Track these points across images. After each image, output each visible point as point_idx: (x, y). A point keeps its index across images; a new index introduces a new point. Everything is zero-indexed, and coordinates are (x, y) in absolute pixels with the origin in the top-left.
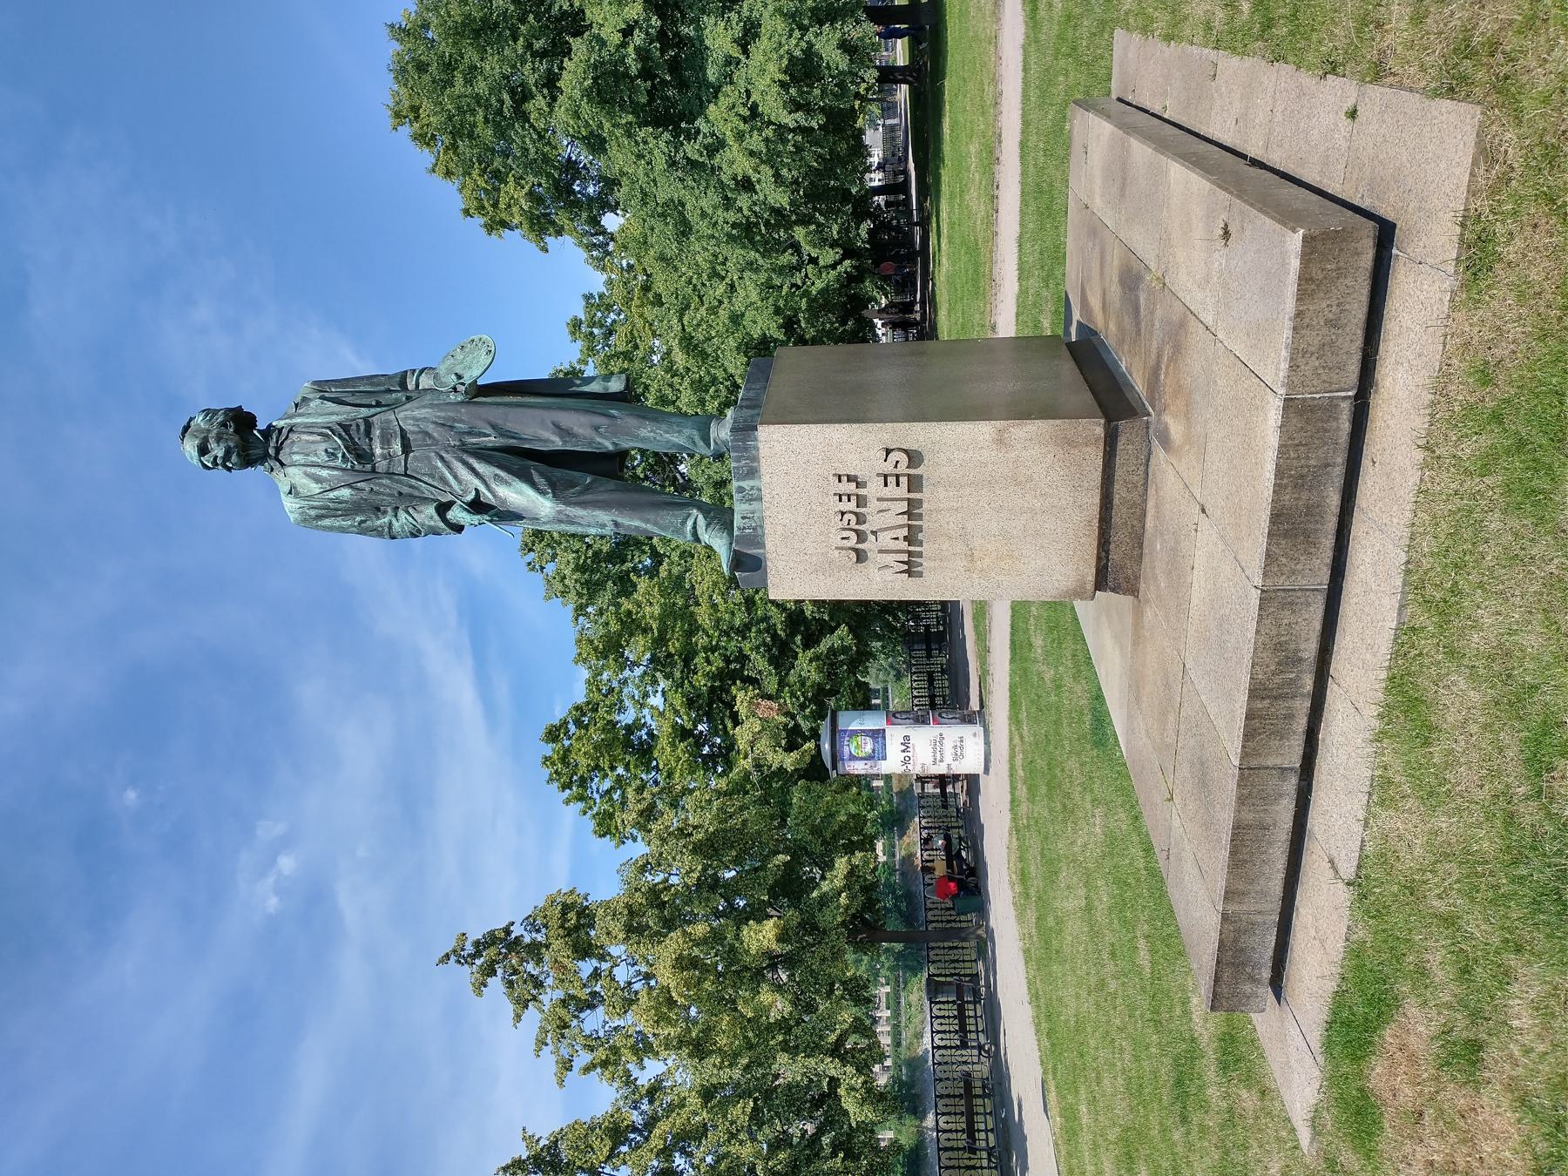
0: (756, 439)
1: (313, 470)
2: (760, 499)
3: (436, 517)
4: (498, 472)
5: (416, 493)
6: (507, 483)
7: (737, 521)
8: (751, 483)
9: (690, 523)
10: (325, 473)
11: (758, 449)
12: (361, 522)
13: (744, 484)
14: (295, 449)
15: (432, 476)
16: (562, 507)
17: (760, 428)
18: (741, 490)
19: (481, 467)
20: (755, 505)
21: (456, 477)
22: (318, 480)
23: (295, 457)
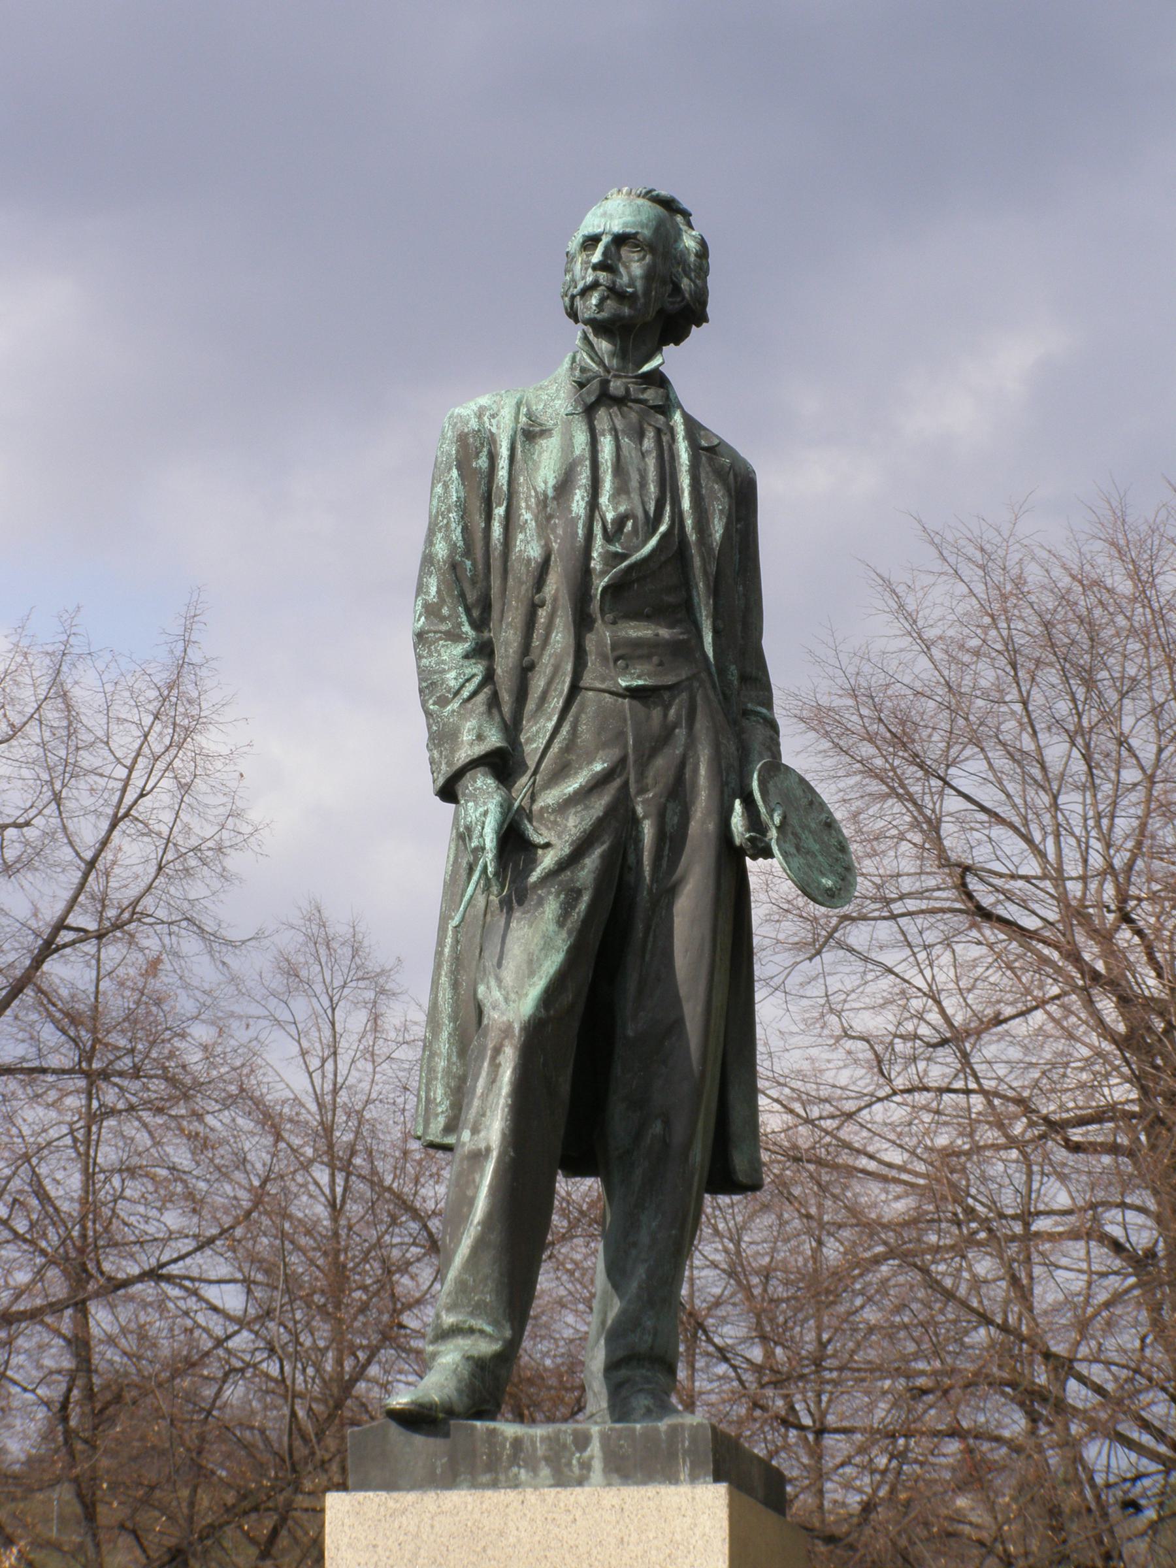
0: (693, 1479)
1: (583, 477)
2: (561, 1480)
3: (479, 750)
4: (586, 898)
5: (531, 705)
6: (561, 921)
8: (597, 1465)
9: (478, 1323)
10: (578, 503)
11: (672, 1479)
13: (595, 1448)
14: (625, 441)
15: (568, 748)
17: (722, 1489)
19: (591, 862)
20: (545, 1472)
22: (564, 487)
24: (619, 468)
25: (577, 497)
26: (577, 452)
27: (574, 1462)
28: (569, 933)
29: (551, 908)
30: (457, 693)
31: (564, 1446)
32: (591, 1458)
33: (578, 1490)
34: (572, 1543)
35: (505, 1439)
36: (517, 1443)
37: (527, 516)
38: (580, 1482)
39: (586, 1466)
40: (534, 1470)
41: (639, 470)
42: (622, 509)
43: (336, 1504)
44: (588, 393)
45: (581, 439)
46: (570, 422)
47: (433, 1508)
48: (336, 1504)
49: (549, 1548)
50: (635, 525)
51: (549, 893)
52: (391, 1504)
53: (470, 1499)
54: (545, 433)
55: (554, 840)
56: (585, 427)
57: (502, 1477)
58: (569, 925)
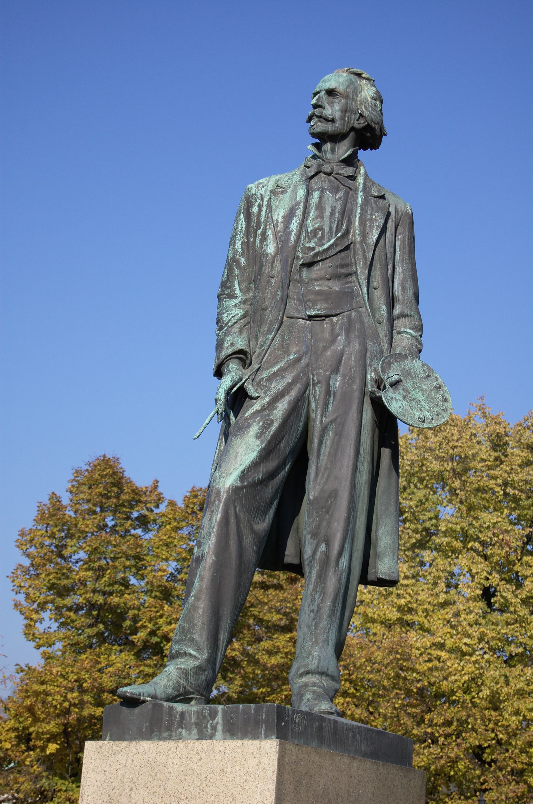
2: (202, 736)
6: (258, 437)
7: (180, 707)
8: (220, 727)
10: (294, 226)
12: (238, 262)
13: (219, 719)
16: (224, 496)
18: (213, 715)
20: (195, 731)
21: (275, 375)
23: (316, 195)
24: (320, 207)
25: (294, 221)
26: (298, 199)
27: (209, 726)
28: (262, 442)
29: (255, 429)
30: (228, 323)
31: (205, 717)
32: (217, 723)
33: (209, 741)
34: (199, 772)
35: (177, 712)
36: (182, 714)
37: (269, 233)
38: (211, 737)
39: (214, 728)
40: (189, 730)
41: (332, 207)
42: (317, 226)
43: (89, 745)
44: (310, 171)
45: (301, 193)
46: (297, 185)
47: (134, 750)
48: (89, 745)
49: (187, 775)
50: (323, 234)
51: (254, 421)
52: (114, 747)
53: (152, 746)
54: (284, 192)
55: (262, 395)
56: (304, 187)
57: (174, 734)
58: (263, 438)
